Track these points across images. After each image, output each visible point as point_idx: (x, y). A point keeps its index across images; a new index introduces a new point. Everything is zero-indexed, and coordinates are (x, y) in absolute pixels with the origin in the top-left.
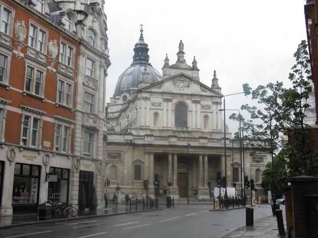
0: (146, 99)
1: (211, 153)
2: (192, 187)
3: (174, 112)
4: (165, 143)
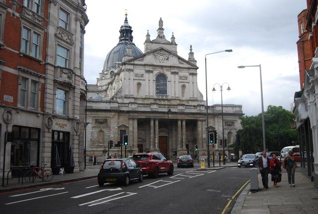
0: (130, 70)
1: (188, 118)
3: (155, 82)
4: (148, 109)
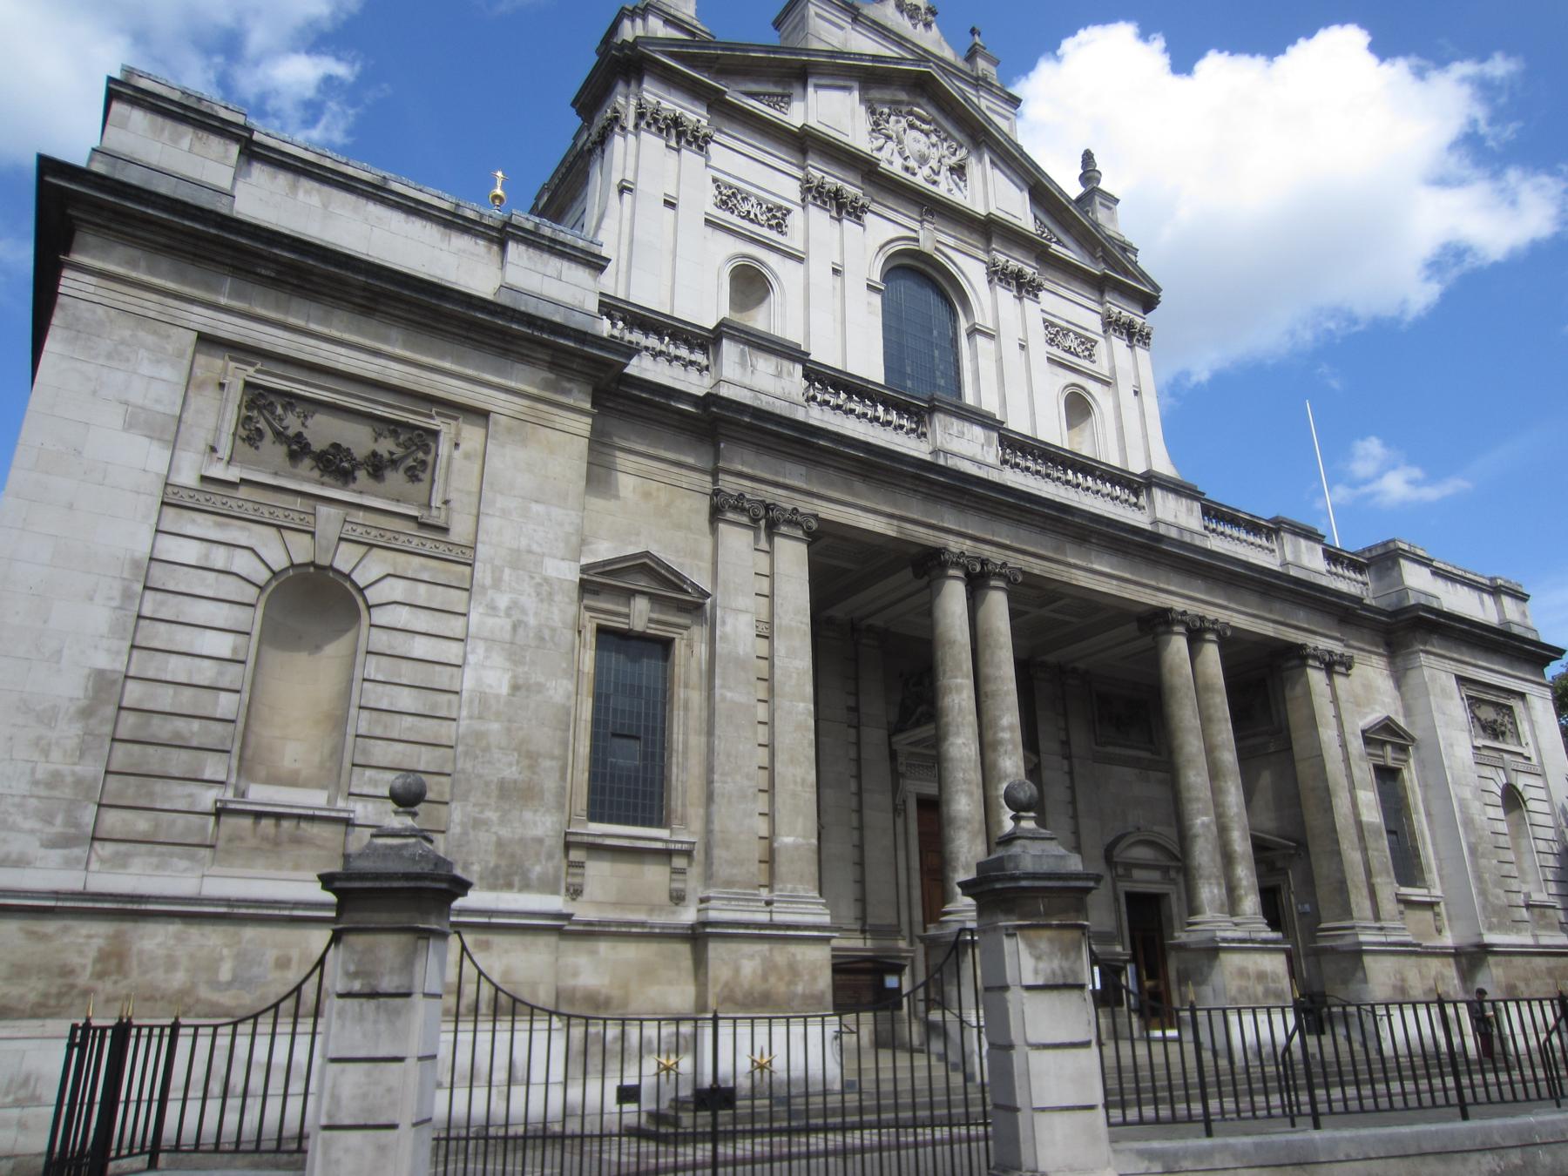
0: (675, 129)
3: (877, 300)
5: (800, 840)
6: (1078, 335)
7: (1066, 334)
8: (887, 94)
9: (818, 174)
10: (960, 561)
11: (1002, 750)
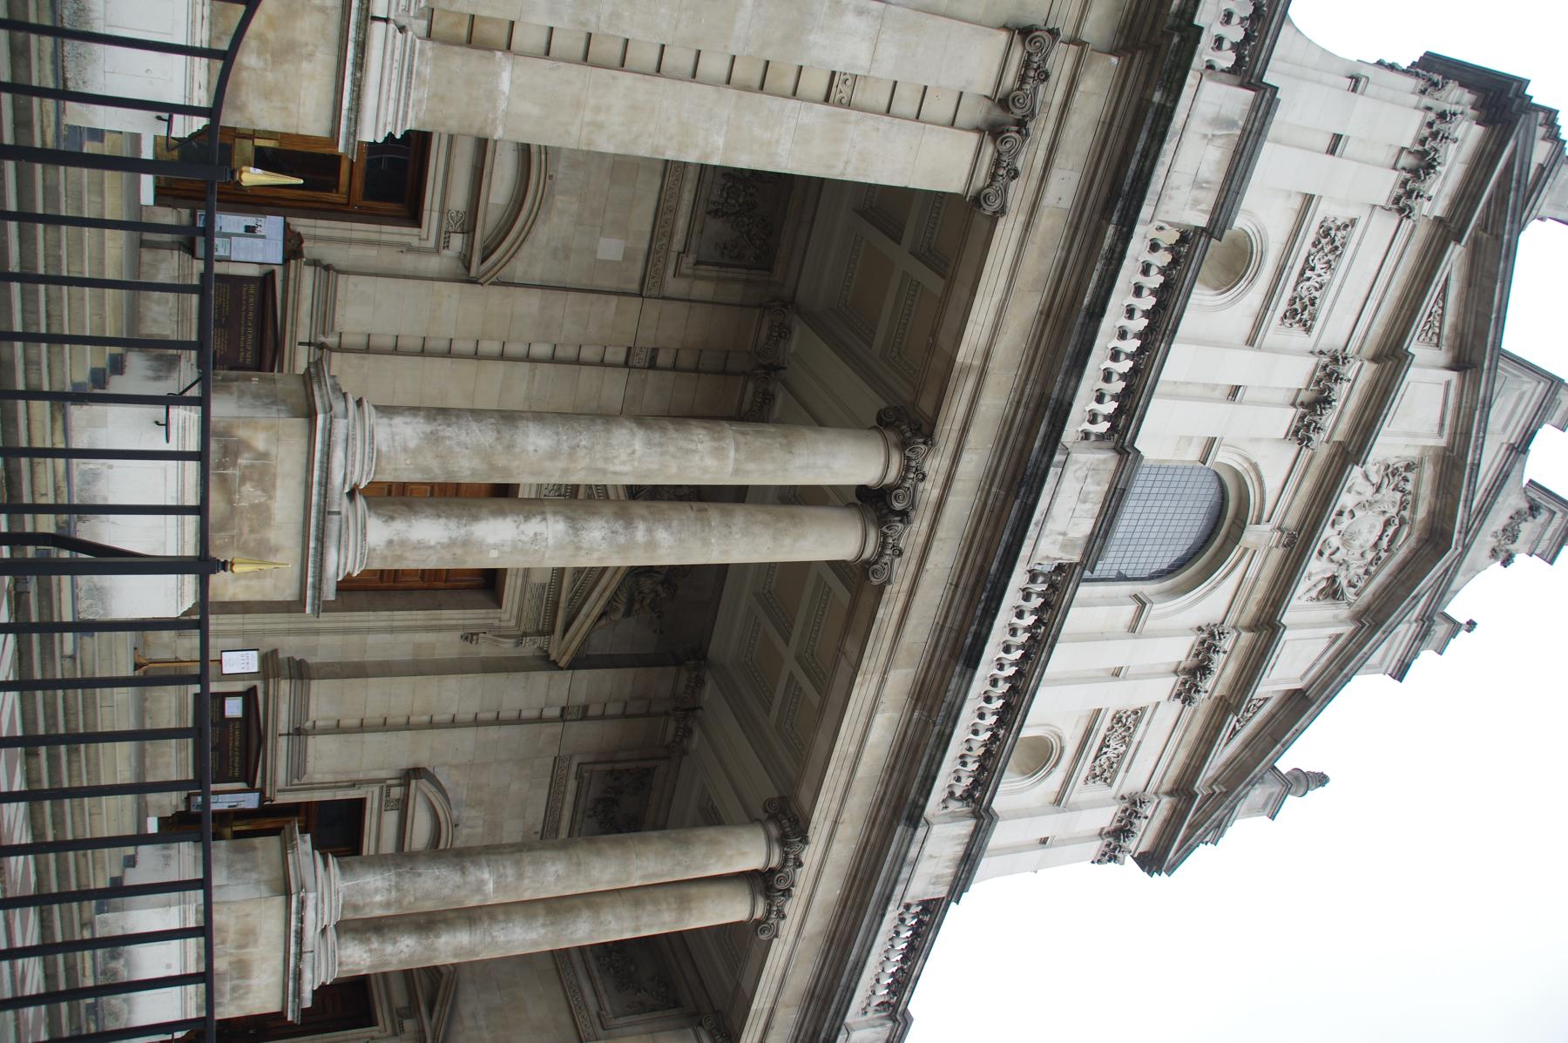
0: (1423, 163)
2: (301, 671)
5: (502, 105)
6: (1121, 756)
7: (1125, 741)
8: (1426, 491)
9: (1351, 375)
10: (913, 472)
11: (618, 526)
